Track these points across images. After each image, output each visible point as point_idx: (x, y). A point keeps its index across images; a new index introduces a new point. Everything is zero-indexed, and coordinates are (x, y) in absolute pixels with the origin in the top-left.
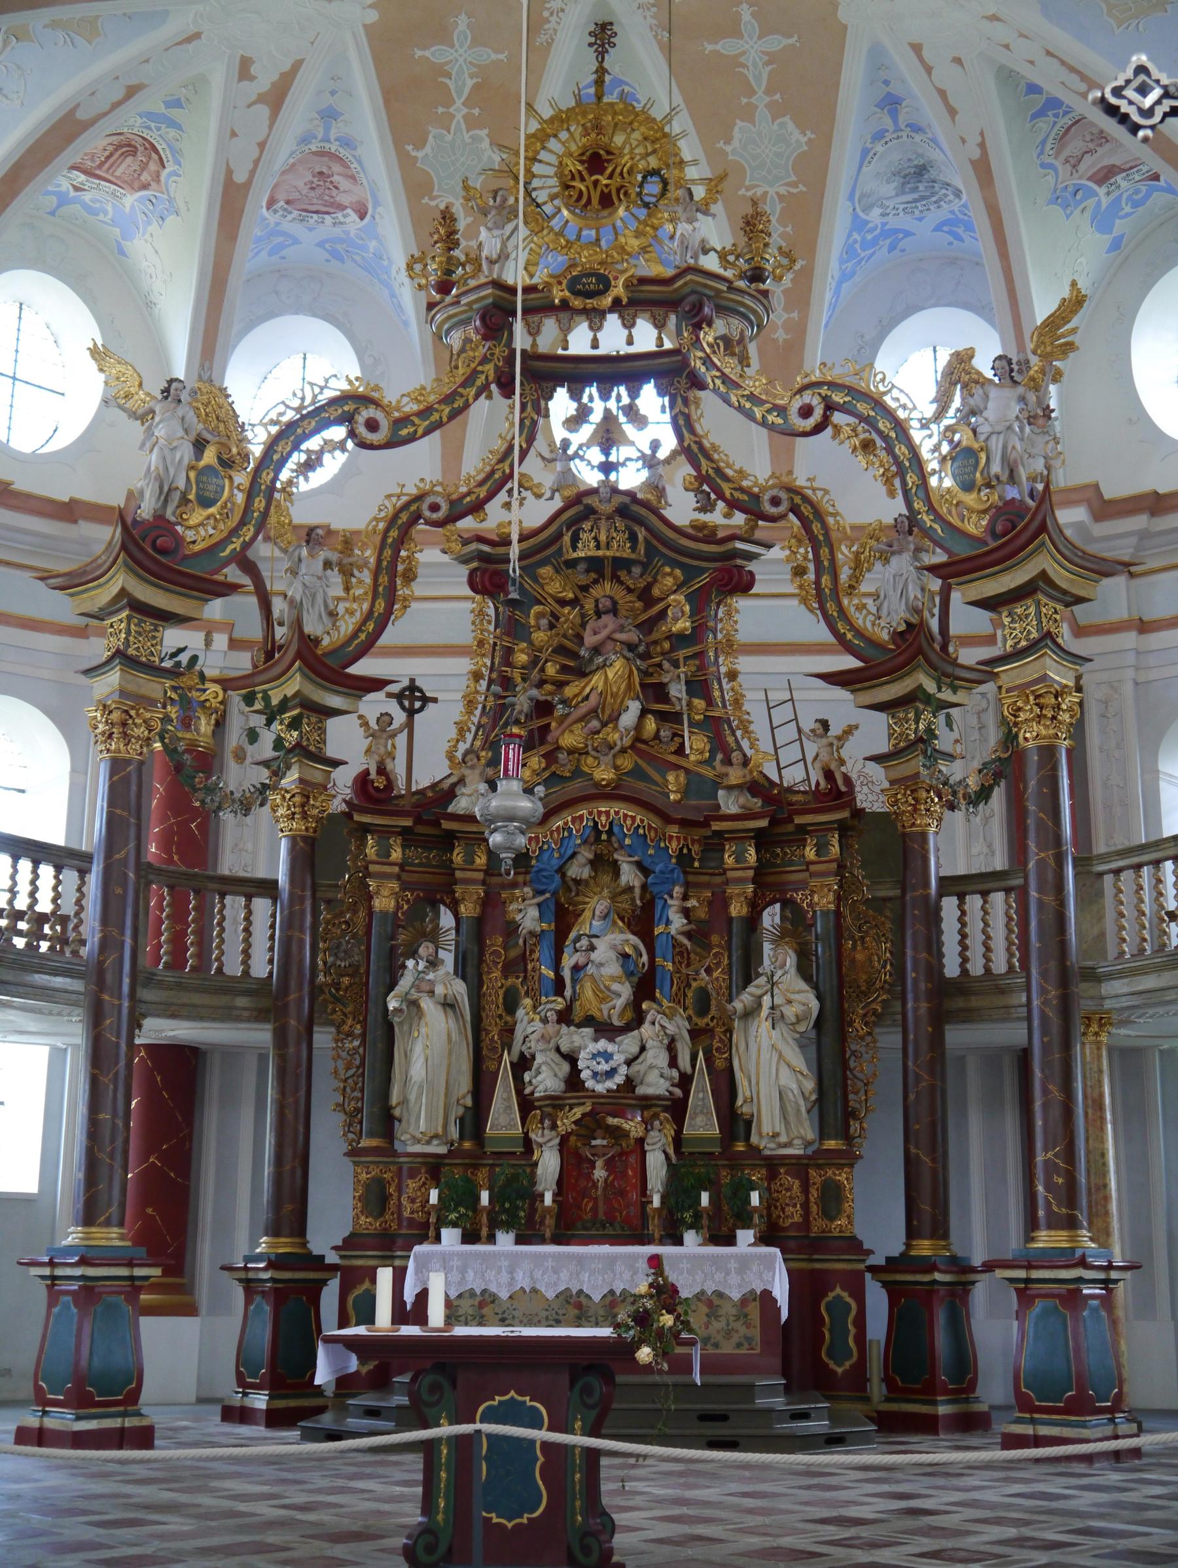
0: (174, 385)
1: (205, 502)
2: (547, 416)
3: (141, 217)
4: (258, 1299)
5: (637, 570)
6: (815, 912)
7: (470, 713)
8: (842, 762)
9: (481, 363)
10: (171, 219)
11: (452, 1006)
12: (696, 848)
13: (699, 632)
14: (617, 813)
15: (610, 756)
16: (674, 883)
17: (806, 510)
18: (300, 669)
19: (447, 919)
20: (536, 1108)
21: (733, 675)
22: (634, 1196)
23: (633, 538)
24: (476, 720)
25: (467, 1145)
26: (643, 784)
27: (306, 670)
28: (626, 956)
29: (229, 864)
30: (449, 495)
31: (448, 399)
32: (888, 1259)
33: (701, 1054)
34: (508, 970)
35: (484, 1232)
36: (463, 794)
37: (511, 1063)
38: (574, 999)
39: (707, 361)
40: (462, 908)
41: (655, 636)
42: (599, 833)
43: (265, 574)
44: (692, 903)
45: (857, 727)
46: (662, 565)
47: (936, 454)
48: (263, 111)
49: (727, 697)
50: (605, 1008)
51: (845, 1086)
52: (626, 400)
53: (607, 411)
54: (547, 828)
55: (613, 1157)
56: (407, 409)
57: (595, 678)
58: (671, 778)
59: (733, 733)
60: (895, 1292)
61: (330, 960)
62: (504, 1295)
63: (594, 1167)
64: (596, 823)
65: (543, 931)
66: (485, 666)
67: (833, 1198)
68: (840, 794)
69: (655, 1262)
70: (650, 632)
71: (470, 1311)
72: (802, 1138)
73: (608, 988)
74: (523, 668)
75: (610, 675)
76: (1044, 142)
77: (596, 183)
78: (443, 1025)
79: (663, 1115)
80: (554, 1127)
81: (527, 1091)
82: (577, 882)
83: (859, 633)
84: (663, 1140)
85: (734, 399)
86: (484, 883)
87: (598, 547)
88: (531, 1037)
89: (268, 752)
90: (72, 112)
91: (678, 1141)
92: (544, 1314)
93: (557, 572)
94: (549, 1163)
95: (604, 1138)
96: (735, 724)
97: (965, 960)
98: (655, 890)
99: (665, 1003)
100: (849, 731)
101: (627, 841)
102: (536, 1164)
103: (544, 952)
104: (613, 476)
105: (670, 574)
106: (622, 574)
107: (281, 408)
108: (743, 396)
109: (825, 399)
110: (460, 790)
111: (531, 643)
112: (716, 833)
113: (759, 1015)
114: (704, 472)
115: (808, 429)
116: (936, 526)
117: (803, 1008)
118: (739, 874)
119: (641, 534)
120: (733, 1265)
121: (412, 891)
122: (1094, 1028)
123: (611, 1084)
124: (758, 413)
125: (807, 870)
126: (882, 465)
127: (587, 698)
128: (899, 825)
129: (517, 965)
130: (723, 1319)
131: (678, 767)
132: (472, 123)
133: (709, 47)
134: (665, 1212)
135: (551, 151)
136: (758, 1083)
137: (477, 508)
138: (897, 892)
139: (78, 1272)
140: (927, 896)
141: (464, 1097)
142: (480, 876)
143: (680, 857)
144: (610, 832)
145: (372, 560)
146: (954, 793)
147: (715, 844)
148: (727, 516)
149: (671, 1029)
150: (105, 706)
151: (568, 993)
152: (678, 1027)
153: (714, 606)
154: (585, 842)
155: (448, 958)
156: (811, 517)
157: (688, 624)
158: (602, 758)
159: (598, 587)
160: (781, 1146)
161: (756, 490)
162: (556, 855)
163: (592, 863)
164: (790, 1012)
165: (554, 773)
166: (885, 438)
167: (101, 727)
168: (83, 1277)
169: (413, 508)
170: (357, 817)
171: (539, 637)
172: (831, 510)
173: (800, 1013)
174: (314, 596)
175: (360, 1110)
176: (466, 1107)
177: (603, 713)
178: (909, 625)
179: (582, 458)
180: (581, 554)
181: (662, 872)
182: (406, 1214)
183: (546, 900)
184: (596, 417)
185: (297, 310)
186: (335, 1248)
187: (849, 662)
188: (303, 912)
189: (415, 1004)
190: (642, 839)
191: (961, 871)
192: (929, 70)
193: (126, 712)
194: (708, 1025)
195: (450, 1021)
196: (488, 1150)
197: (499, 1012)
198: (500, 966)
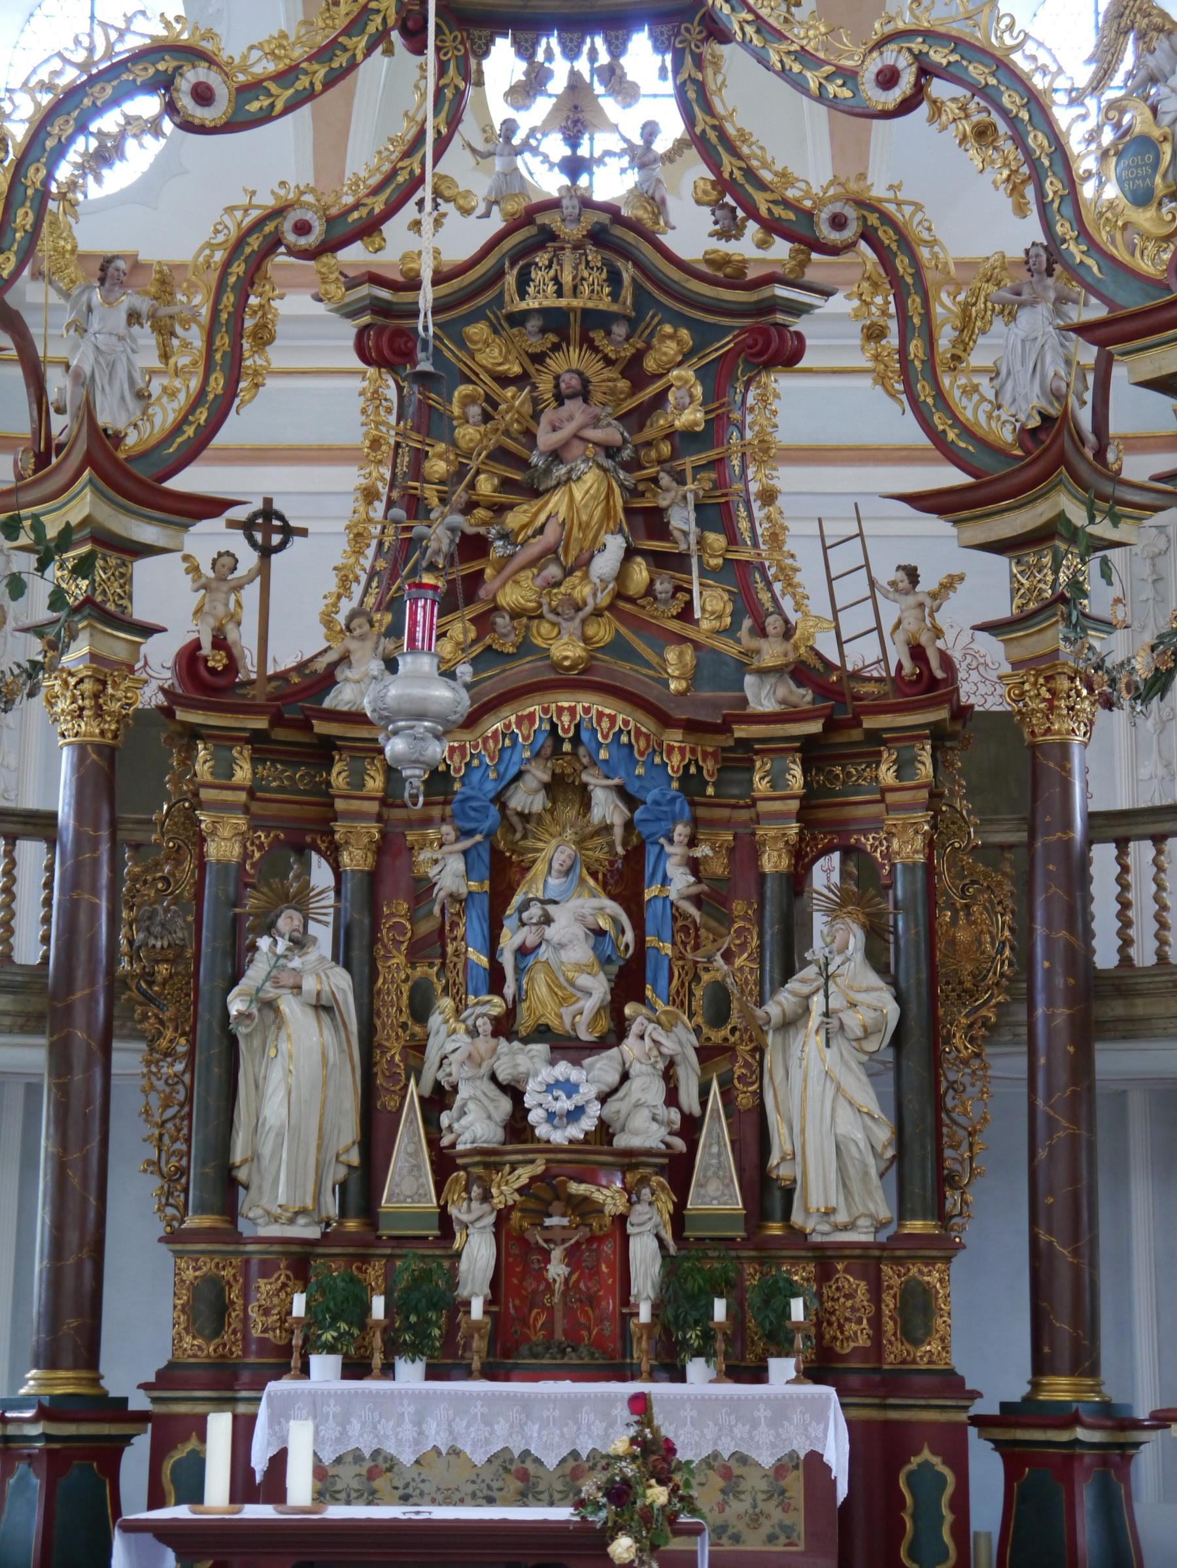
2: (480, 83)
5: (620, 330)
6: (893, 866)
7: (359, 553)
8: (938, 633)
11: (328, 1009)
12: (709, 766)
14: (587, 710)
15: (577, 621)
16: (675, 820)
17: (886, 236)
18: (90, 481)
19: (321, 875)
20: (458, 1168)
21: (769, 496)
22: (610, 1305)
23: (614, 279)
24: (367, 564)
25: (352, 1225)
26: (628, 666)
27: (100, 483)
28: (599, 933)
30: (326, 208)
31: (323, 54)
32: (1004, 1406)
33: (715, 1086)
34: (416, 952)
35: (377, 1360)
36: (347, 680)
37: (422, 1099)
38: (518, 999)
40: (345, 858)
41: (648, 434)
42: (559, 741)
43: (35, 331)
44: (703, 851)
45: (961, 578)
46: (659, 323)
47: (1093, 146)
49: (759, 531)
50: (567, 1012)
51: (939, 1136)
52: (604, 58)
54: (478, 731)
55: (578, 1244)
56: (258, 70)
57: (555, 499)
58: (671, 655)
59: (769, 586)
61: (139, 937)
62: (407, 1458)
63: (548, 1261)
64: (554, 726)
65: (470, 893)
66: (382, 479)
68: (934, 683)
69: (640, 1404)
70: (641, 428)
71: (355, 1485)
72: (871, 1216)
73: (572, 983)
74: (441, 482)
75: (578, 495)
78: (315, 1039)
79: (656, 1180)
80: (486, 1197)
81: (445, 1142)
82: (525, 817)
83: (967, 431)
84: (656, 1219)
85: (774, 58)
86: (379, 818)
87: (559, 293)
88: (452, 1058)
89: (41, 613)
91: (678, 1220)
92: (470, 1488)
93: (496, 331)
95: (564, 1215)
96: (771, 572)
97: (1127, 942)
98: (645, 830)
99: (660, 1006)
100: (950, 584)
101: (603, 754)
102: (458, 1255)
103: (473, 927)
104: (583, 181)
105: (671, 337)
106: (598, 336)
107: (57, 64)
108: (789, 53)
109: (918, 57)
110: (341, 673)
111: (454, 443)
112: (739, 741)
113: (806, 1026)
114: (726, 175)
115: (891, 106)
116: (1090, 262)
117: (873, 1014)
119: (628, 272)
120: (762, 1413)
121: (267, 830)
123: (576, 1131)
124: (812, 80)
125: (882, 801)
126: (1006, 165)
127: (541, 530)
128: (1026, 731)
130: (747, 1498)
131: (683, 640)
134: (657, 1330)
136: (803, 1131)
137: (370, 229)
138: (1023, 836)
140: (1068, 844)
141: (347, 1150)
142: (374, 807)
143: (685, 778)
144: (576, 740)
145: (205, 312)
146: (1113, 682)
148: (762, 244)
149: (669, 1046)
151: (509, 989)
152: (680, 1043)
153: (740, 387)
154: (537, 755)
155: (323, 934)
156: (894, 247)
157: (700, 415)
158: (564, 624)
159: (559, 355)
160: (837, 1228)
161: (808, 204)
162: (492, 775)
163: (547, 787)
164: (854, 1021)
165: (489, 648)
166: (1012, 120)
169: (269, 228)
170: (181, 715)
171: (467, 434)
172: (925, 235)
173: (869, 1022)
174: (112, 366)
175: (183, 1171)
176: (350, 1167)
177: (566, 555)
178: (1045, 417)
179: (535, 151)
180: (532, 303)
181: (656, 803)
182: (256, 1333)
183: (475, 846)
184: (558, 84)
186: (145, 1386)
187: (952, 477)
188: (96, 862)
190: (626, 751)
191: (1123, 803)
194: (726, 1039)
195: (326, 1032)
196: (384, 1232)
197: (402, 1019)
198: (404, 947)
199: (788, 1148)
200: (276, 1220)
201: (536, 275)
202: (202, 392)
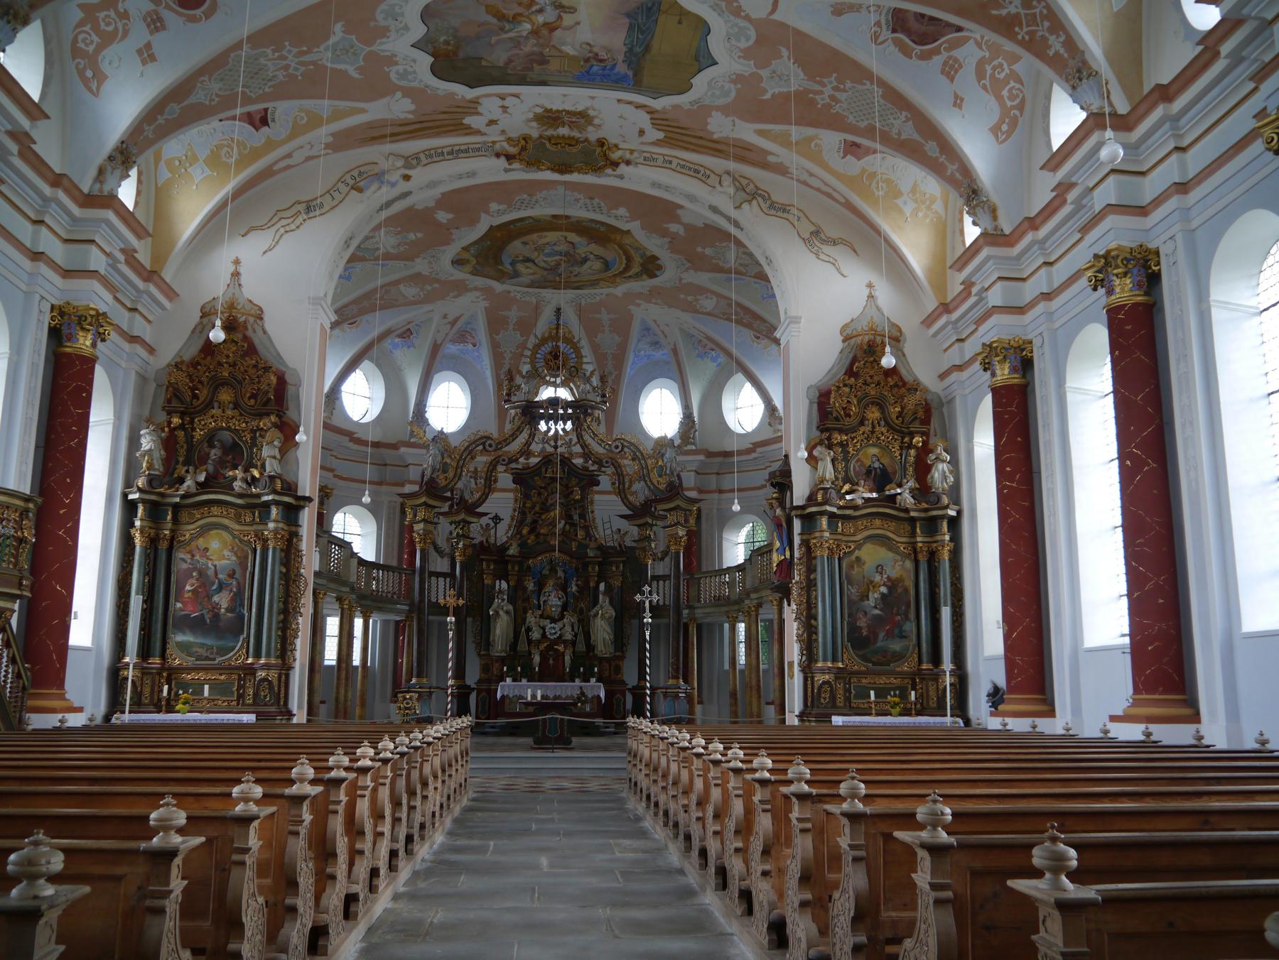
1: (445, 472)
13: (583, 498)
21: (592, 512)
39: (589, 427)
48: (449, 326)
53: (557, 431)
60: (634, 696)
67: (618, 669)
83: (630, 503)
91: (574, 652)
94: (537, 659)
100: (627, 532)
129: (527, 600)
137: (516, 461)
147: (586, 565)
155: (505, 597)
164: (607, 615)
185: (449, 369)
189: (497, 613)
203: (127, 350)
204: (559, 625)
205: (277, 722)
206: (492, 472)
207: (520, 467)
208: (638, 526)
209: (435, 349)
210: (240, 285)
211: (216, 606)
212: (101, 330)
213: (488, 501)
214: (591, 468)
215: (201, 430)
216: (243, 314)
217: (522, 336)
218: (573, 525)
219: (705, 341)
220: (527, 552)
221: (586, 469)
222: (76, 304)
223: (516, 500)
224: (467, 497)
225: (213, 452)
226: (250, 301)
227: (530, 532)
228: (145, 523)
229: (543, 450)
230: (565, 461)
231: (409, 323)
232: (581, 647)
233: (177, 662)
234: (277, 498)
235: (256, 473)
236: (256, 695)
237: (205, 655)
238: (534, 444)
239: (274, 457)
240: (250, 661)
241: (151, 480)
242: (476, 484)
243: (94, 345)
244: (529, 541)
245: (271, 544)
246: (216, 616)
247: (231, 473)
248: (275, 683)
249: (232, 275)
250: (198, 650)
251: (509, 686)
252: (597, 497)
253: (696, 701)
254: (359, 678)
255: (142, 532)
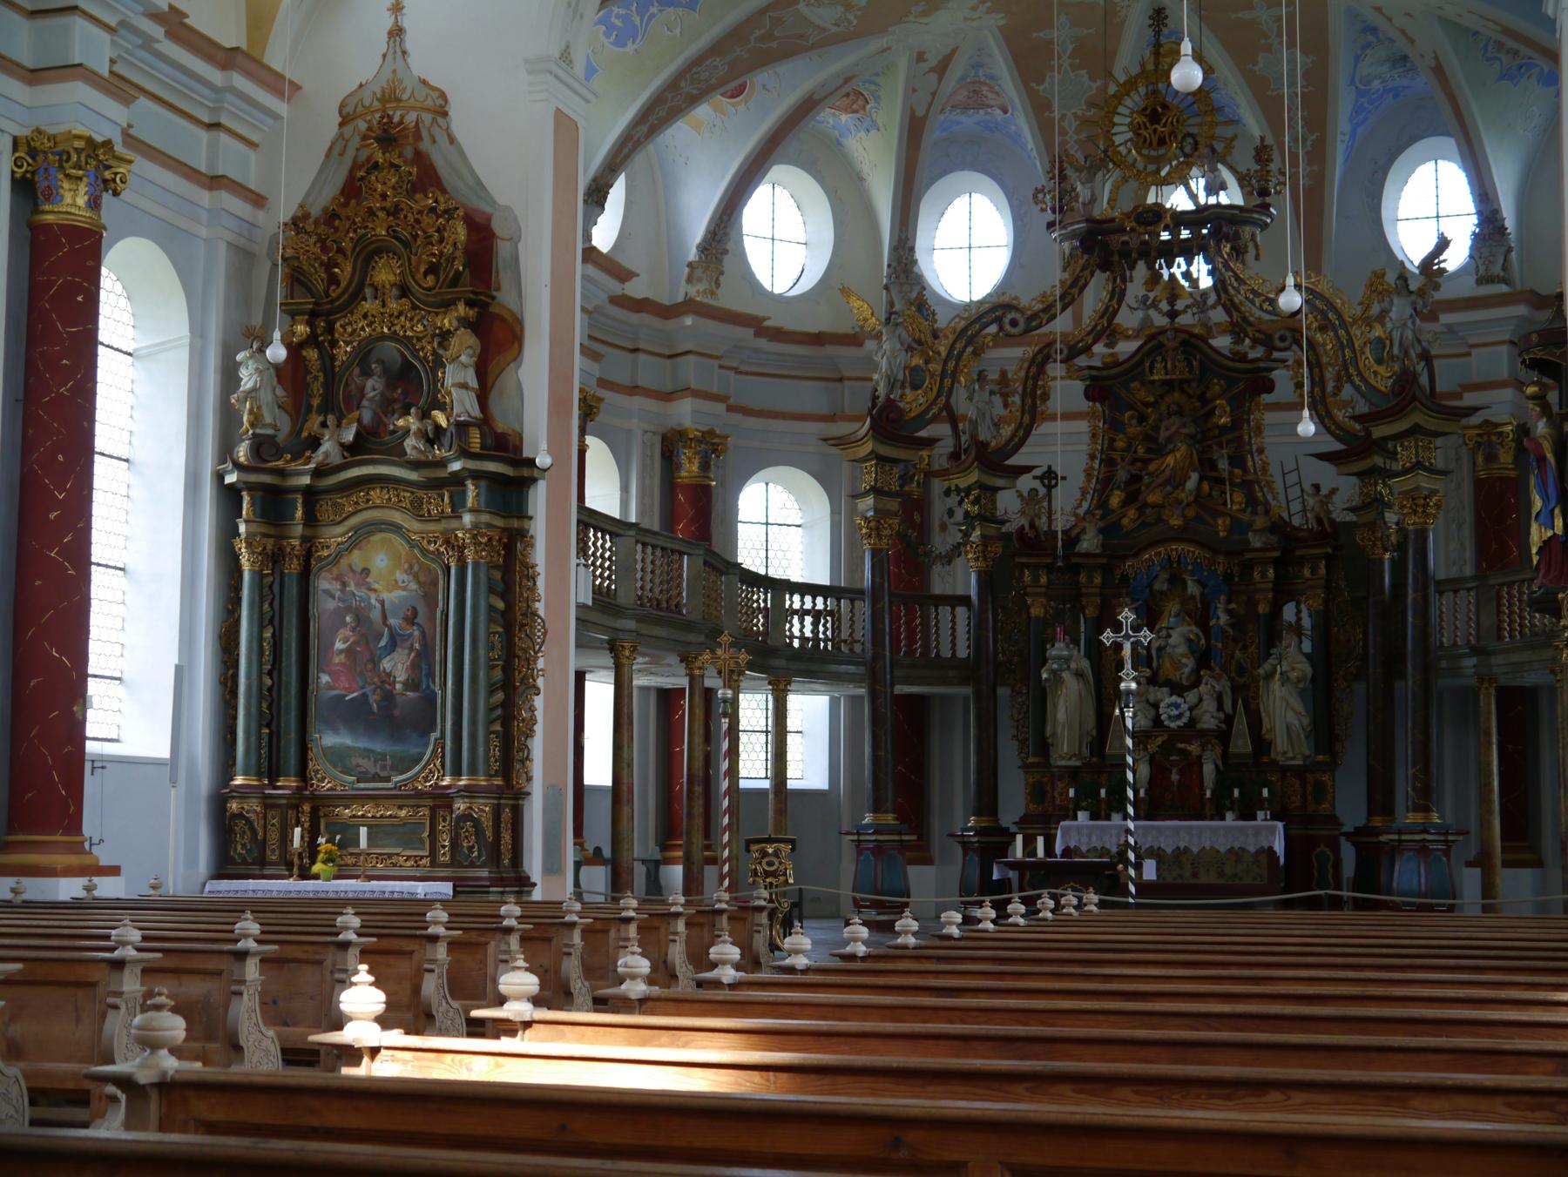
0: (893, 317)
1: (915, 387)
3: (853, 128)
4: (971, 853)
5: (1194, 384)
8: (1328, 512)
9: (1082, 271)
10: (873, 132)
12: (1236, 570)
13: (1237, 423)
18: (977, 467)
21: (1261, 451)
23: (1190, 365)
24: (1092, 486)
28: (1190, 640)
29: (937, 588)
32: (1356, 828)
33: (1240, 702)
35: (1103, 813)
38: (1159, 666)
40: (1087, 611)
44: (1233, 606)
48: (934, 77)
50: (1178, 674)
52: (1184, 268)
56: (1035, 308)
58: (1220, 522)
59: (1262, 490)
61: (1006, 646)
64: (1169, 556)
67: (1320, 791)
76: (1486, 48)
77: (1155, 130)
79: (1214, 741)
80: (1146, 749)
82: (1161, 593)
83: (1338, 426)
87: (1167, 374)
90: (811, 96)
91: (1225, 756)
100: (1334, 491)
101: (1190, 568)
105: (1217, 384)
107: (957, 320)
118: (1263, 586)
122: (1486, 685)
123: (1180, 723)
127: (1164, 471)
131: (1224, 514)
132: (1074, 68)
133: (1233, 16)
135: (1126, 106)
137: (1087, 349)
139: (873, 838)
144: (1179, 562)
145: (1020, 390)
147: (1247, 567)
149: (1218, 688)
150: (866, 518)
151: (1155, 664)
167: (864, 531)
168: (875, 841)
169: (1045, 351)
171: (1131, 431)
174: (984, 414)
175: (1027, 739)
182: (1058, 802)
186: (1015, 823)
188: (987, 618)
192: (1390, 20)
193: (878, 521)
199: (1269, 727)
200: (1063, 758)
201: (1158, 365)
202: (1021, 423)
203: (206, 204)
204: (1192, 697)
205: (492, 898)
206: (1036, 379)
207: (1099, 364)
208: (1358, 475)
209: (914, 131)
210: (404, 53)
211: (388, 678)
212: (108, 175)
213: (1030, 440)
214: (1252, 355)
215: (347, 343)
216: (413, 108)
217: (1092, 78)
218: (1219, 481)
219: (1510, 43)
220: (1117, 544)
221: (1242, 358)
222: (51, 130)
223: (1094, 436)
224: (983, 435)
225: (370, 383)
226: (424, 82)
227: (1126, 503)
228: (254, 528)
229: (1147, 321)
230: (1192, 344)
231: (847, 81)
232: (1242, 744)
233: (327, 785)
234: (472, 465)
235: (441, 418)
236: (455, 844)
237: (372, 771)
238: (1124, 309)
239: (464, 386)
240: (447, 781)
241: (262, 447)
242: (1006, 406)
243: (94, 204)
244: (1125, 521)
245: (470, 555)
246: (388, 698)
247: (401, 423)
248: (487, 822)
249: (390, 34)
250: (361, 761)
251: (1079, 829)
252: (1270, 417)
253: (1498, 861)
254: (771, 813)
255: (249, 545)
